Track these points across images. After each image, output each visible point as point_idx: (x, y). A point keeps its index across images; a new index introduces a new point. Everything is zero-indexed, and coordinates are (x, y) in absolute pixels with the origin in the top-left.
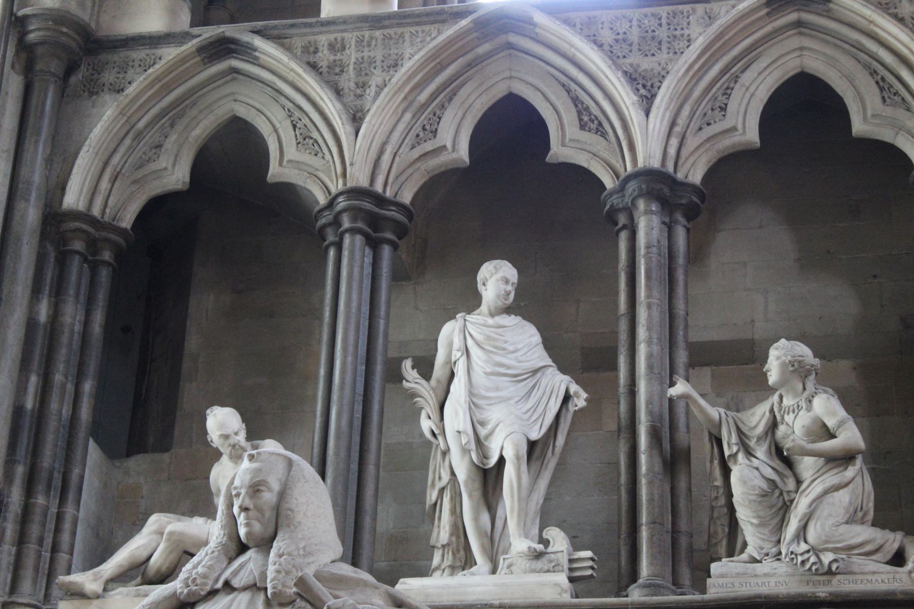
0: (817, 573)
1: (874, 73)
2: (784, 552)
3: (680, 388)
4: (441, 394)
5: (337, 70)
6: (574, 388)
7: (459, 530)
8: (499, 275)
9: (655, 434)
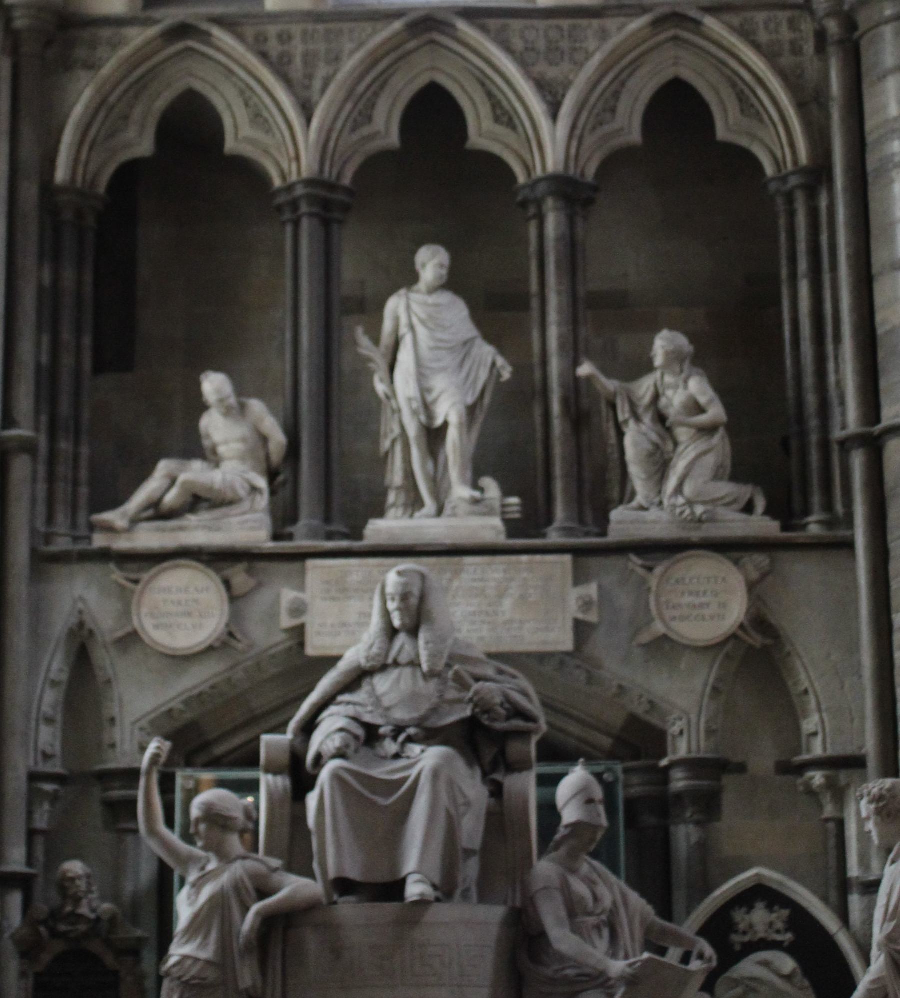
0: (691, 521)
1: (734, 86)
2: (666, 502)
3: (585, 369)
4: (390, 357)
5: (286, 60)
6: (500, 361)
7: (409, 474)
8: (436, 261)
9: (565, 402)
